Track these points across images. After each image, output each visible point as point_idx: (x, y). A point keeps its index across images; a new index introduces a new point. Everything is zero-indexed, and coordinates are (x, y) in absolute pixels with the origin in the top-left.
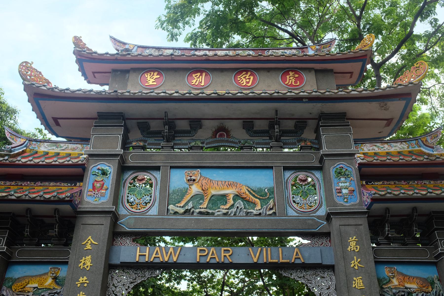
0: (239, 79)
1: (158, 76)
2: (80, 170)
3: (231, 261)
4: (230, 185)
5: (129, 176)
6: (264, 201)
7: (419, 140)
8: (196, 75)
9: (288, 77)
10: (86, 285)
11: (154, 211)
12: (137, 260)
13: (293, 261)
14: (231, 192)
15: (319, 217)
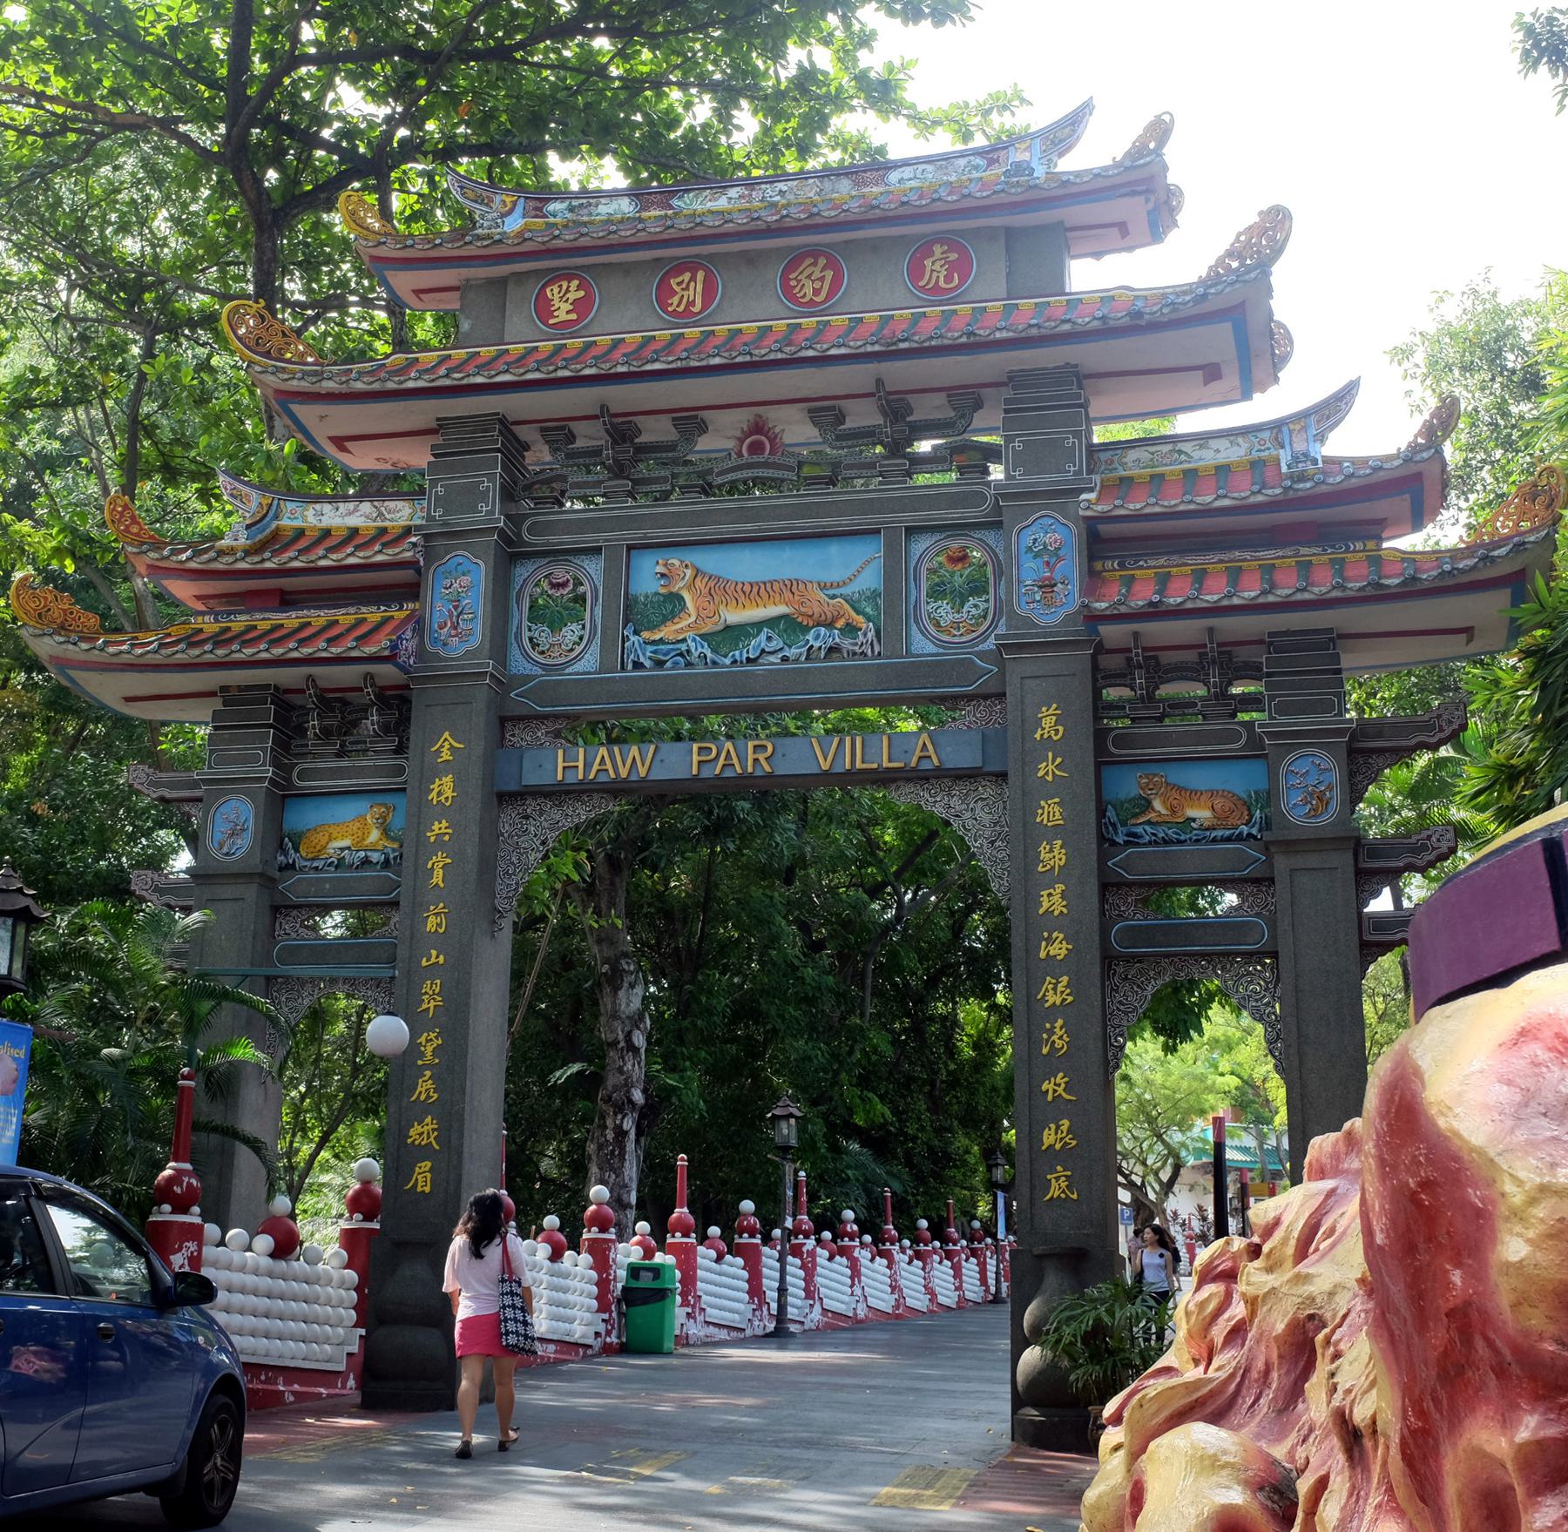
0: (793, 283)
1: (582, 293)
2: (406, 575)
3: (768, 769)
7: (1285, 429)
8: (679, 279)
9: (928, 263)
10: (447, 838)
11: (589, 662)
12: (560, 777)
13: (913, 764)
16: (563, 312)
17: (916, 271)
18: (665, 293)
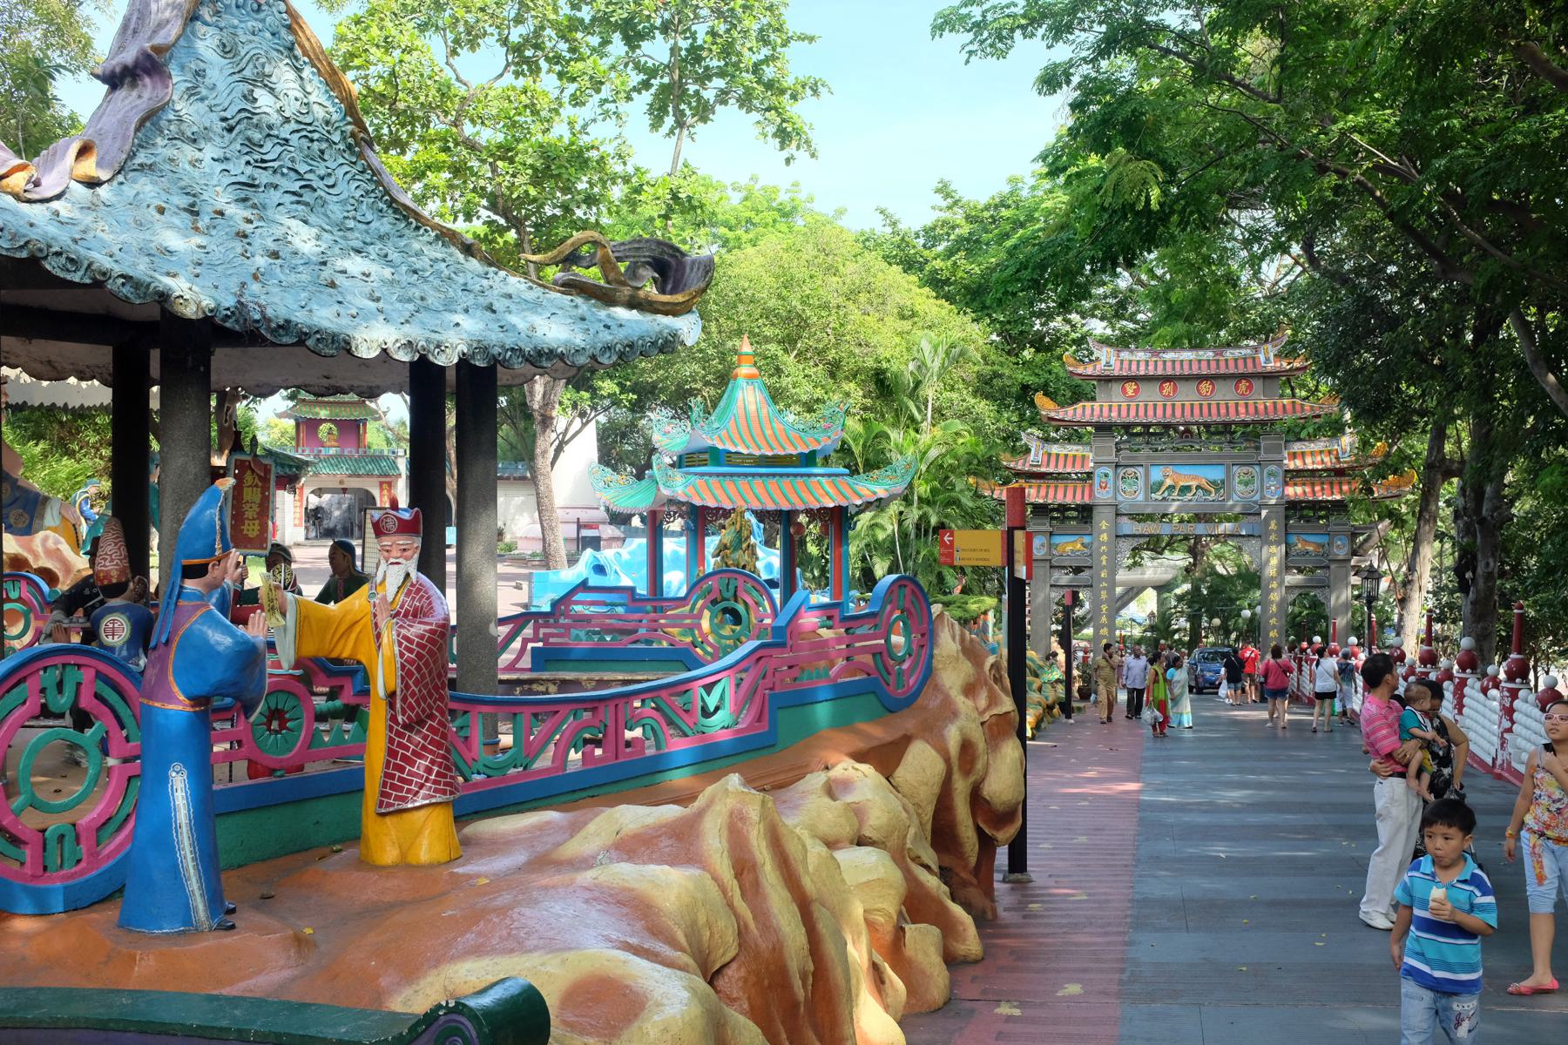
4: (1195, 478)
5: (1121, 472)
6: (1217, 491)
11: (1141, 497)
14: (1194, 484)
15: (1255, 502)
16: (1130, 392)
17: (1237, 388)
18: (1161, 389)
